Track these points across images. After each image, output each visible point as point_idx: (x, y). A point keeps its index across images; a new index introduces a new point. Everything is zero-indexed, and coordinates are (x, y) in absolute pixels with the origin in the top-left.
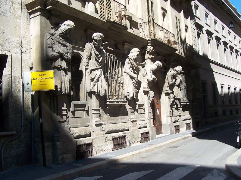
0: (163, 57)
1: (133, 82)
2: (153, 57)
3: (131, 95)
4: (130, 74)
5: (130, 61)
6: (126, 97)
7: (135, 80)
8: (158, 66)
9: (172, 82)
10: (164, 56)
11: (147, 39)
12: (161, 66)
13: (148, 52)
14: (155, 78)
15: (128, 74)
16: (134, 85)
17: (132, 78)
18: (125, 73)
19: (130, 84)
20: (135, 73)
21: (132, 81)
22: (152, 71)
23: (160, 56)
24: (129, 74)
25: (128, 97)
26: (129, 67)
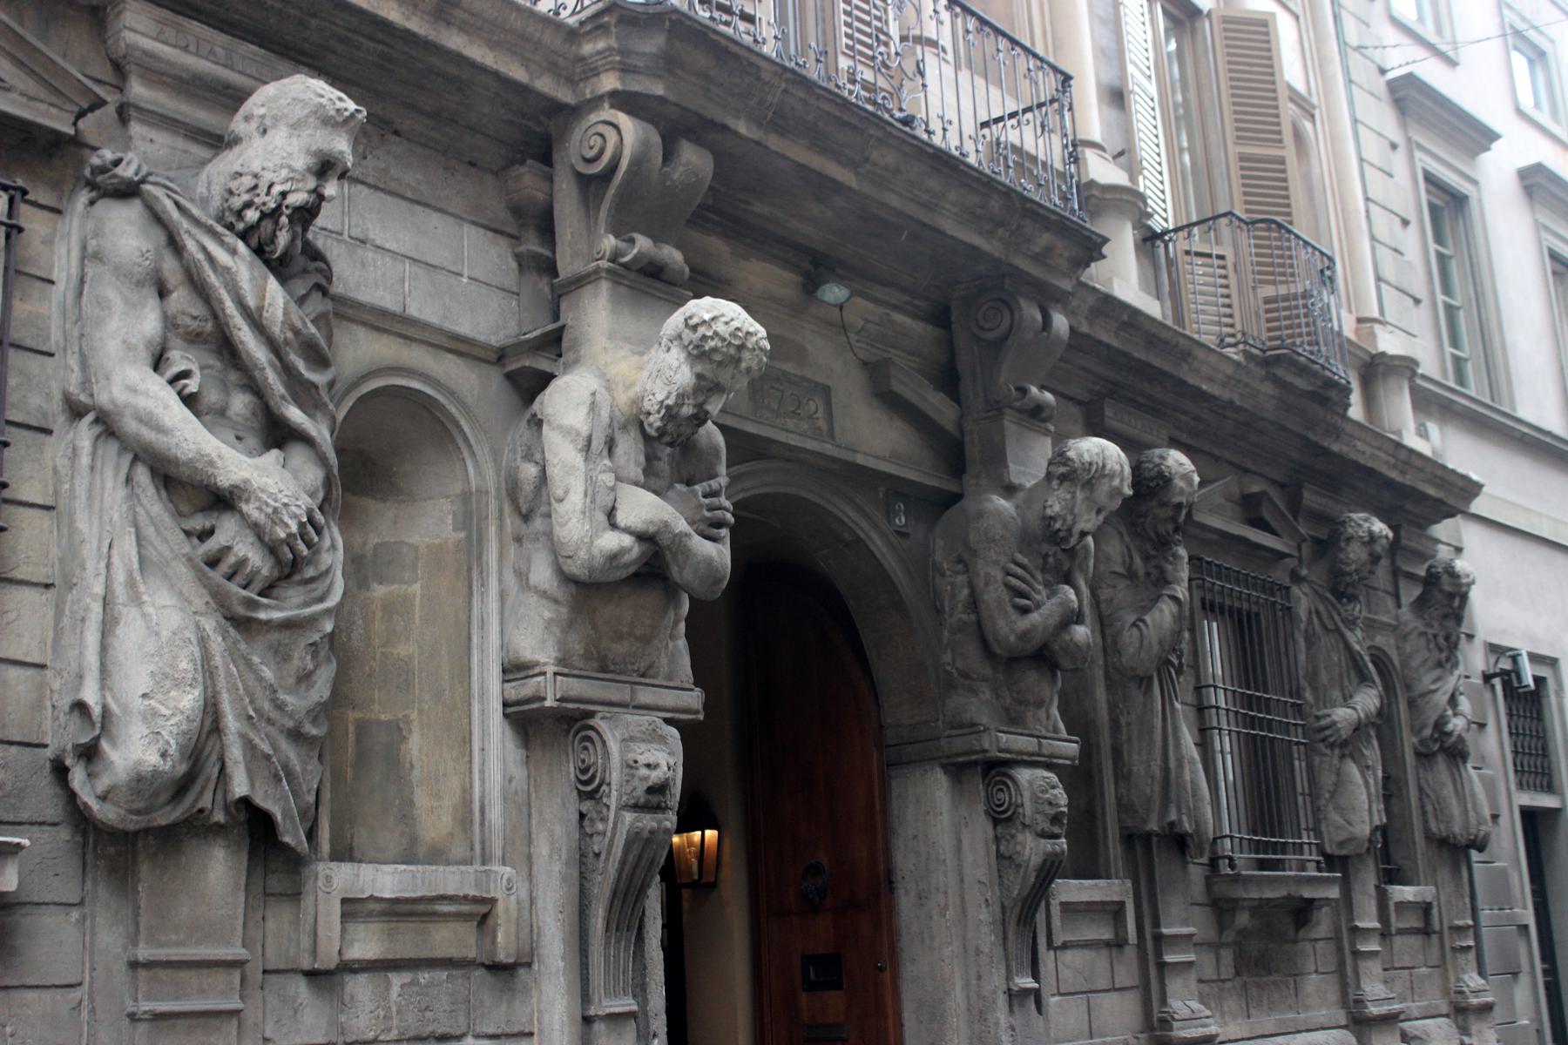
0: (898, 317)
1: (213, 562)
2: (672, 255)
3: (138, 751)
4: (148, 435)
5: (174, 244)
6: (60, 771)
7: (257, 530)
8: (699, 354)
9: (1023, 623)
10: (940, 317)
11: (572, 21)
12: (748, 360)
13: (592, 185)
14: (681, 525)
15: (107, 426)
16: (220, 600)
17: (200, 497)
18: (76, 411)
19: (131, 584)
20: (276, 434)
21: (206, 534)
22: (630, 450)
23: (834, 293)
24: (130, 425)
25: (77, 778)
26: (149, 323)
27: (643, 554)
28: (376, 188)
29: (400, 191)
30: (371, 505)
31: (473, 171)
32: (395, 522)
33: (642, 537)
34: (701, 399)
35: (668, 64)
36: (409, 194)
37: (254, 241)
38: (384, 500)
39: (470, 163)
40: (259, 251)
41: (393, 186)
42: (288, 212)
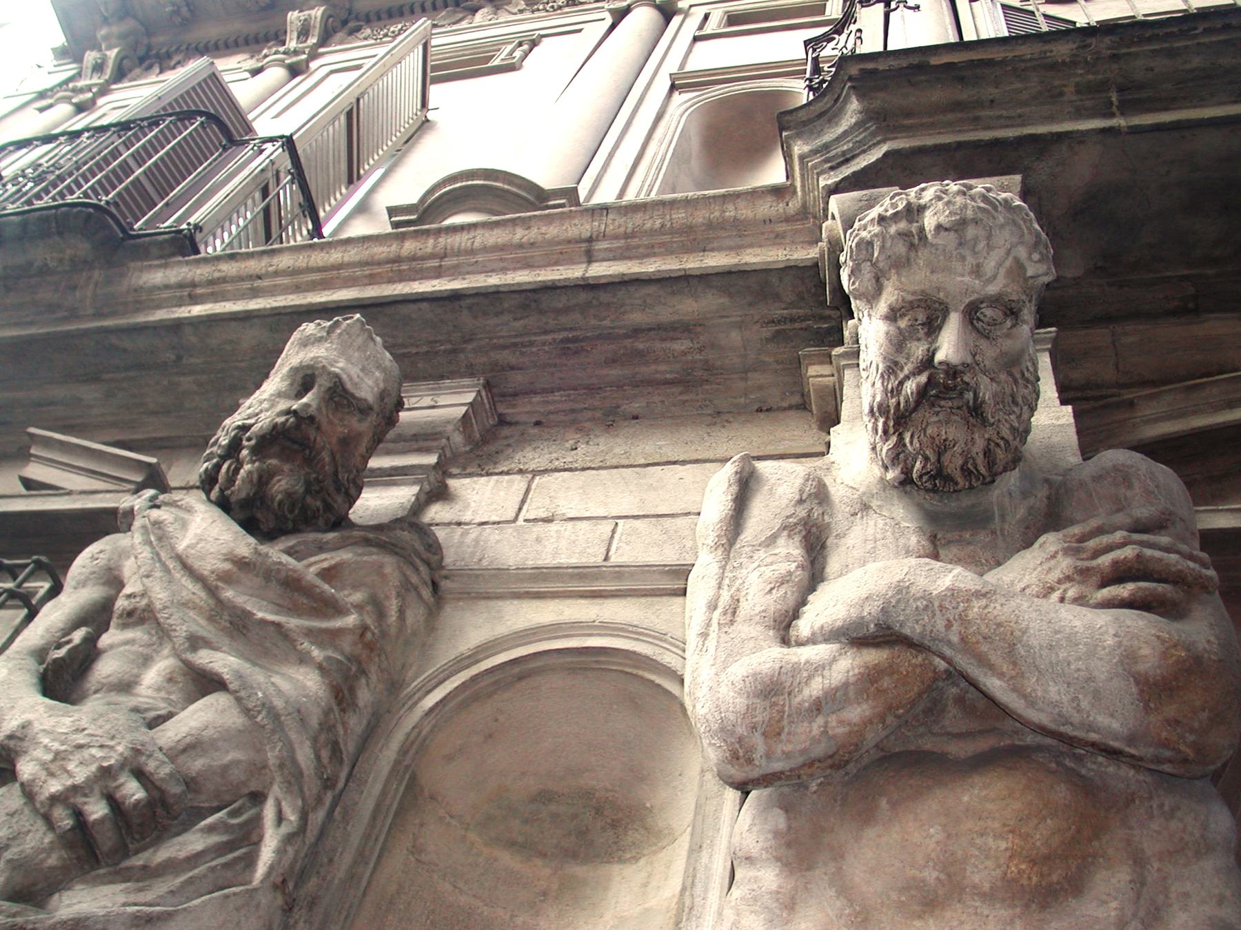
27: (870, 679)
28: (583, 469)
29: (626, 462)
30: (616, 868)
31: (762, 415)
32: (645, 885)
33: (856, 636)
34: (918, 350)
35: (881, 121)
36: (642, 461)
37: (214, 494)
38: (636, 859)
39: (760, 410)
40: (224, 504)
41: (614, 462)
42: (253, 442)
